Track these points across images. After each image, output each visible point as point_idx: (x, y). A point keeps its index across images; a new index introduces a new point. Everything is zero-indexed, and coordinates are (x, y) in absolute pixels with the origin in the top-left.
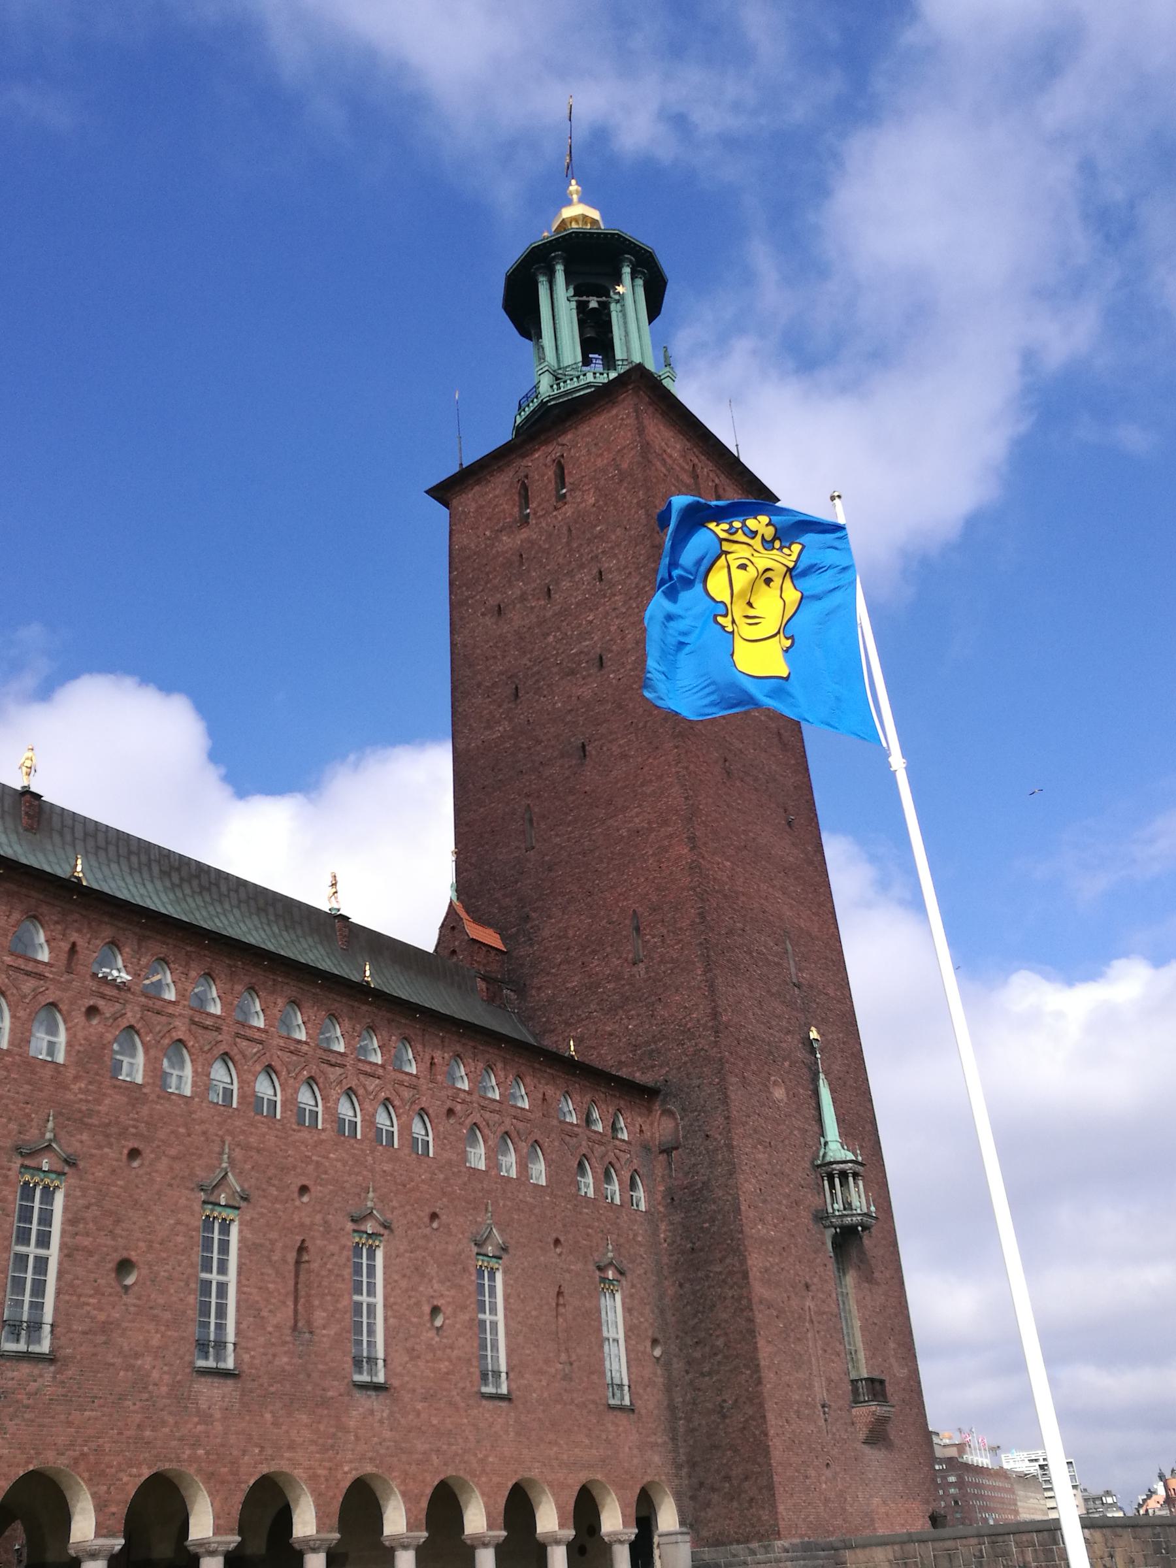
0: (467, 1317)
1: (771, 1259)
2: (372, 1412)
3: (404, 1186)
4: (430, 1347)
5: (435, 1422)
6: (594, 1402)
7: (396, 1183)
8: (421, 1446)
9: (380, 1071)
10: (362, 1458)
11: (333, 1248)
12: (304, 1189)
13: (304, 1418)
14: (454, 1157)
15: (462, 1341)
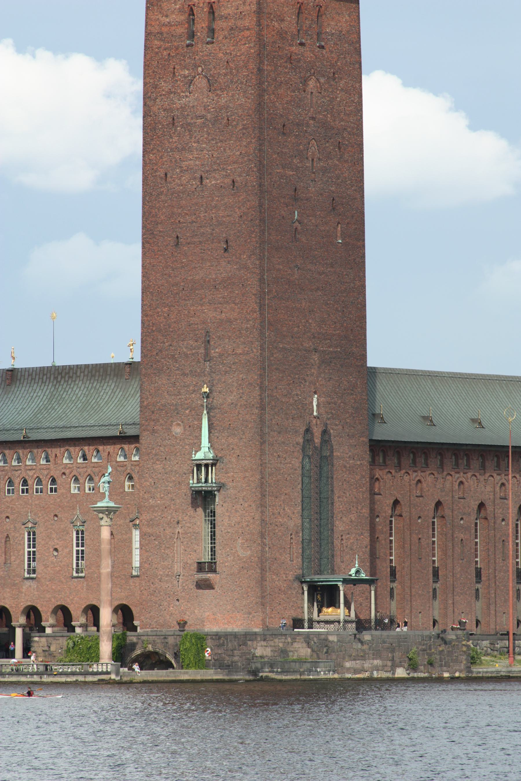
0: (68, 550)
1: (156, 515)
2: (30, 586)
3: (44, 507)
4: (52, 563)
5: (53, 587)
6: (124, 575)
7: (40, 507)
8: (48, 596)
9: (34, 467)
10: (27, 600)
11: (17, 535)
12: (8, 517)
13: (8, 590)
14: (64, 491)
15: (66, 559)
